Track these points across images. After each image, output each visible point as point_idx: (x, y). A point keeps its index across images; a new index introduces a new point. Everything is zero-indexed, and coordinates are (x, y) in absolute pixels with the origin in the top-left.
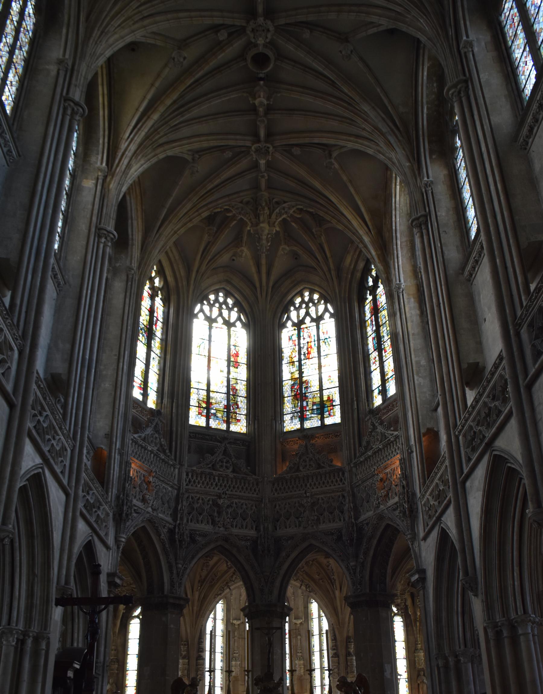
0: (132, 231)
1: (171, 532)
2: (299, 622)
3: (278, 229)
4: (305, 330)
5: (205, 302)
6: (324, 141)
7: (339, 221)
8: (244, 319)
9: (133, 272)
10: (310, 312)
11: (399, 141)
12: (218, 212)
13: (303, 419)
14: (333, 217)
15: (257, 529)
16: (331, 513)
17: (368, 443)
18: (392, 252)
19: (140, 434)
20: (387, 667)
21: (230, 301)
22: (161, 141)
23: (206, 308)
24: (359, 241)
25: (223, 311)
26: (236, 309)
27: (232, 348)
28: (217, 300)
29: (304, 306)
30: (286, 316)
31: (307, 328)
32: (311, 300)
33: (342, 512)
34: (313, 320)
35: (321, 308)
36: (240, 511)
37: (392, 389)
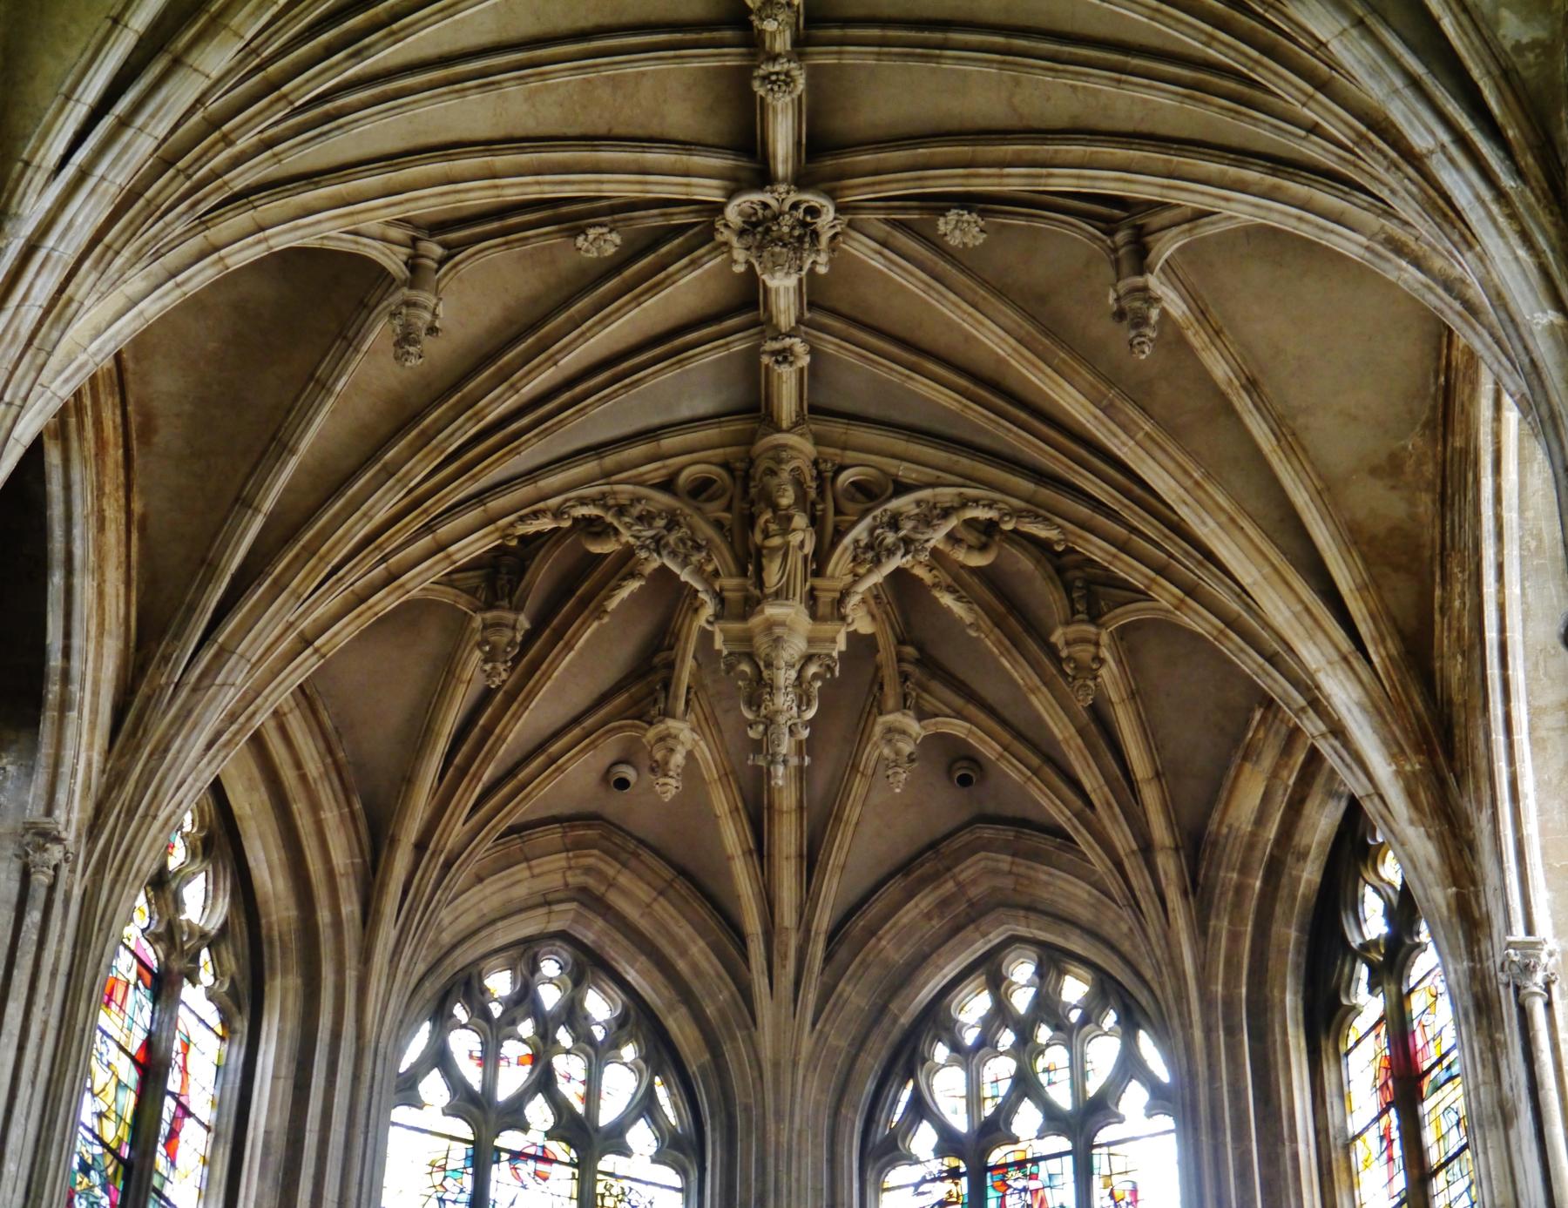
0: (67, 635)
3: (864, 626)
4: (1016, 1180)
5: (460, 1012)
6: (1109, 183)
7: (1191, 591)
8: (675, 1106)
9: (56, 853)
10: (1043, 1078)
11: (1501, 195)
12: (538, 534)
14: (1162, 571)
18: (1483, 765)
21: (599, 1007)
22: (240, 179)
23: (464, 1044)
24: (1302, 702)
25: (560, 1063)
26: (629, 1052)
28: (524, 999)
29: (1007, 1038)
30: (906, 1095)
31: (1020, 1165)
32: (1047, 1007)
34: (1054, 1121)
35: (1103, 1053)
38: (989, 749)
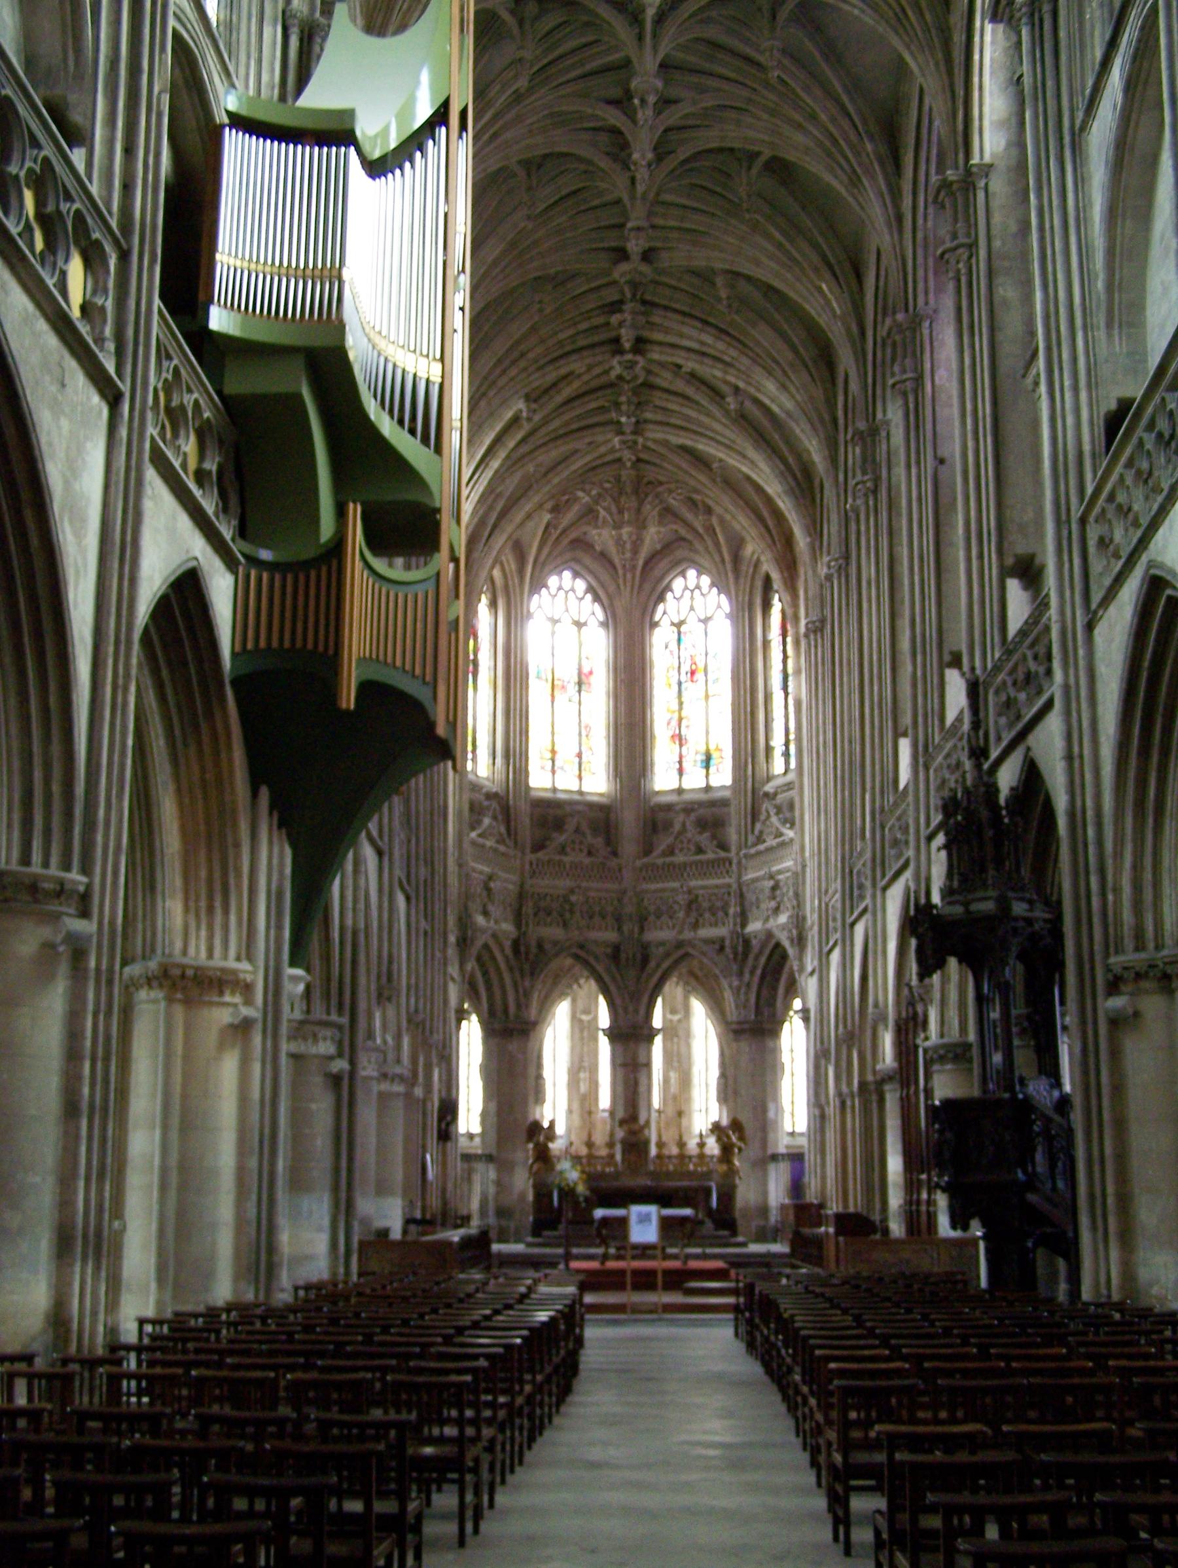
1: (516, 944)
2: (676, 1018)
13: (681, 771)
15: (620, 929)
16: (714, 914)
17: (761, 832)
19: (479, 831)
20: (771, 1107)
27: (584, 662)
29: (688, 593)
32: (698, 587)
33: (727, 914)
36: (597, 909)
37: (793, 765)
38: (683, 532)
